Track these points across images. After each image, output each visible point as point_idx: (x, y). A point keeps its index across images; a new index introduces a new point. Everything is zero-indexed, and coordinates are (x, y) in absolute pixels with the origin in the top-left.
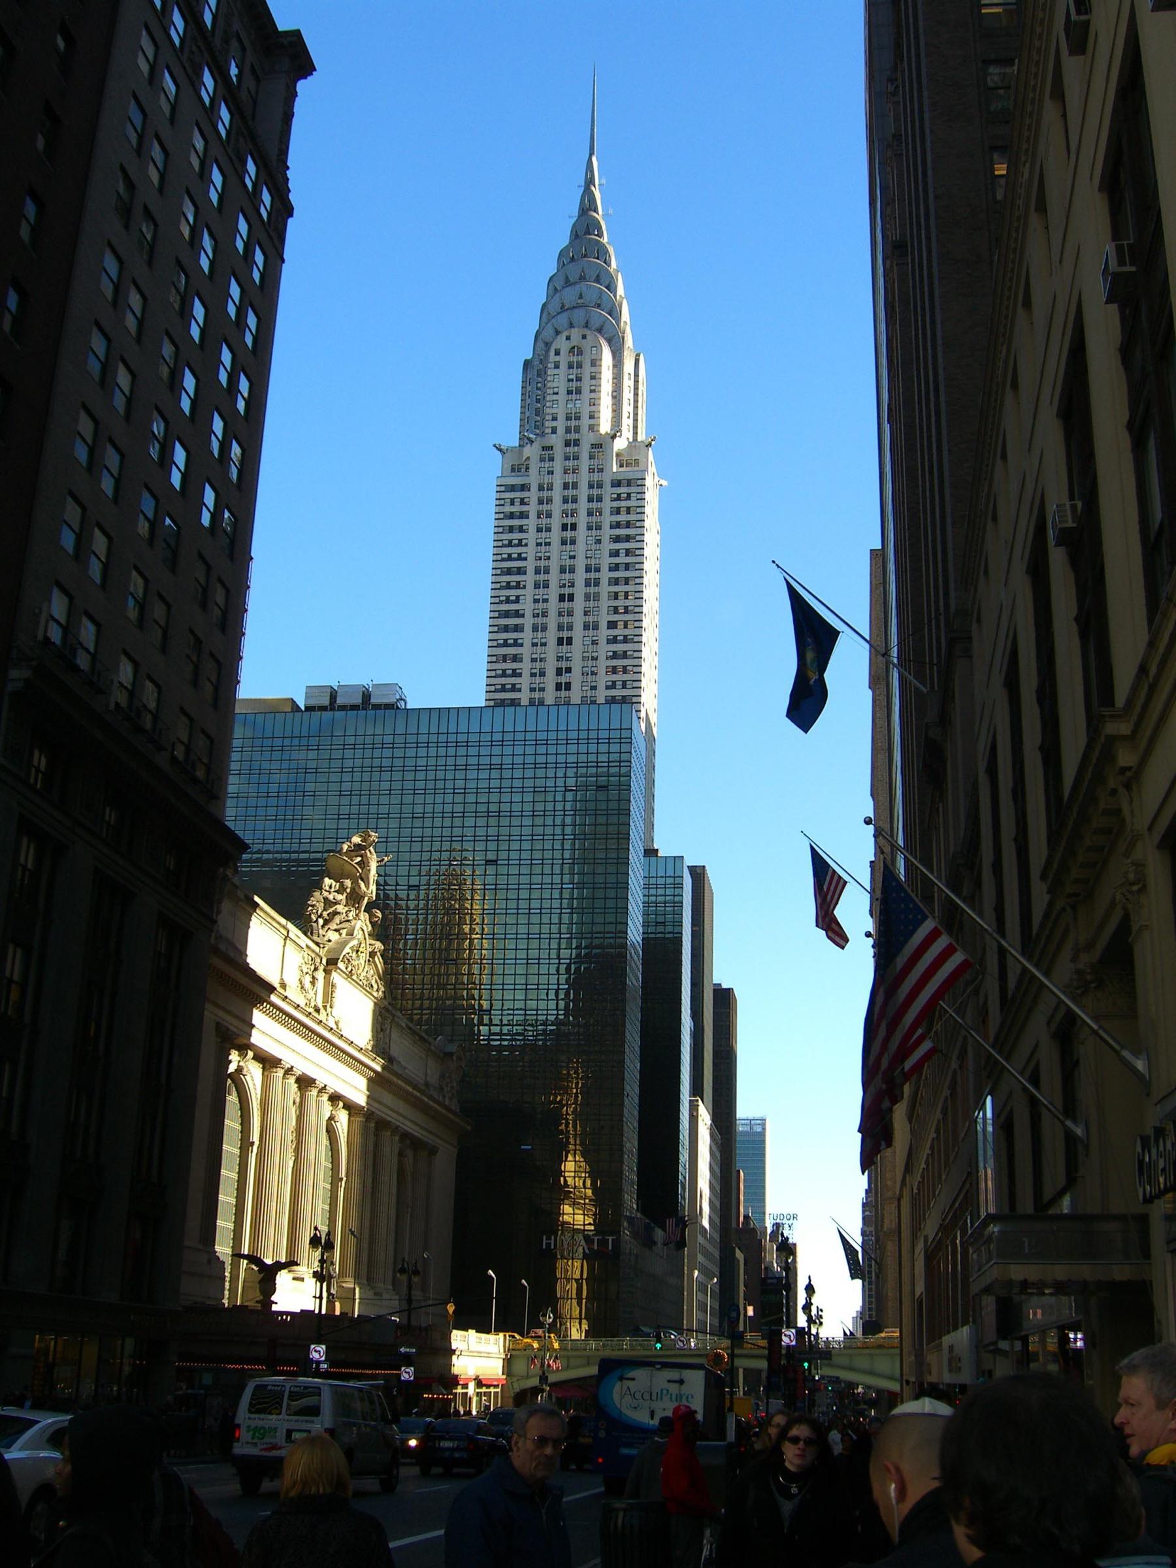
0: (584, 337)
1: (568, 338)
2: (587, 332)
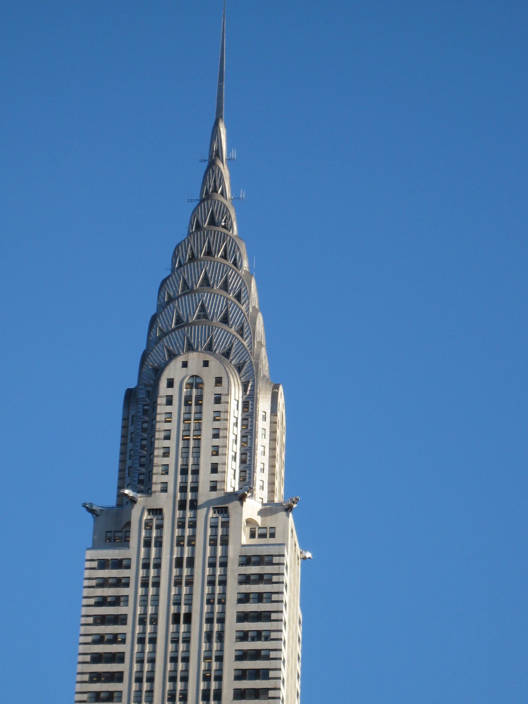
0: (206, 364)
1: (185, 365)
2: (208, 357)
